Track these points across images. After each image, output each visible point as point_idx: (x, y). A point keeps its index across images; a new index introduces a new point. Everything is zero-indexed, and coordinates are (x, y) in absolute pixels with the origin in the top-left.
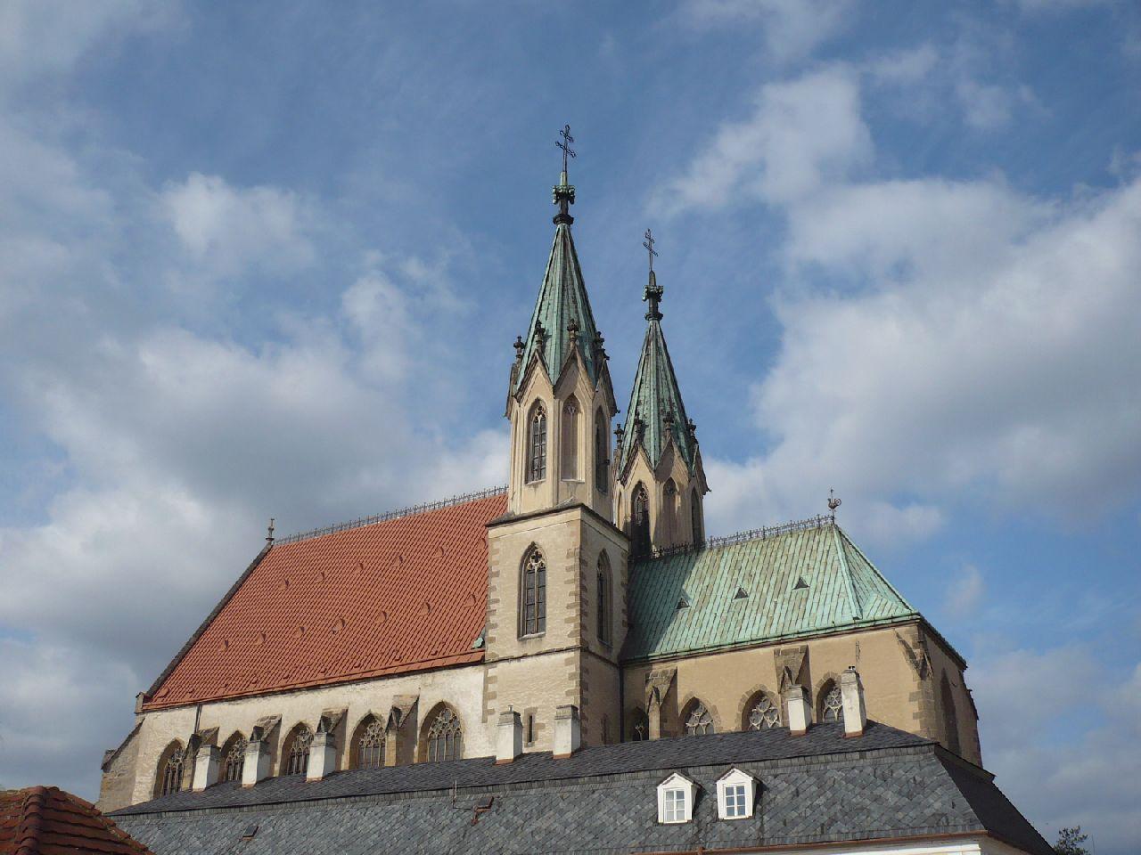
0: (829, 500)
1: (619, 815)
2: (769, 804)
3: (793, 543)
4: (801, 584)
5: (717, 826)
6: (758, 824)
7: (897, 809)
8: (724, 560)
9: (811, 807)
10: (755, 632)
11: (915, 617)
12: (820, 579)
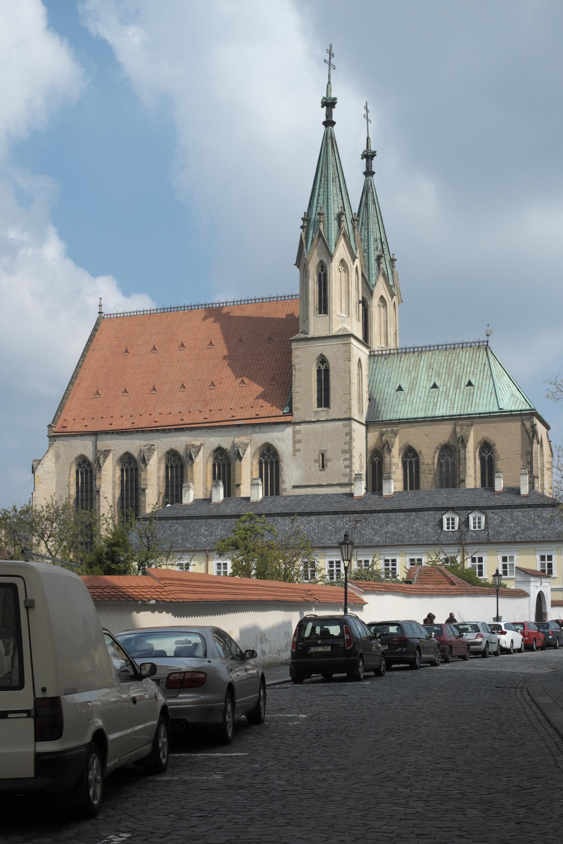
0: (486, 330)
1: (425, 527)
2: (491, 525)
3: (464, 355)
4: (470, 384)
5: (469, 533)
6: (487, 533)
7: (543, 529)
8: (422, 361)
9: (508, 527)
10: (444, 412)
11: (533, 411)
12: (480, 382)
